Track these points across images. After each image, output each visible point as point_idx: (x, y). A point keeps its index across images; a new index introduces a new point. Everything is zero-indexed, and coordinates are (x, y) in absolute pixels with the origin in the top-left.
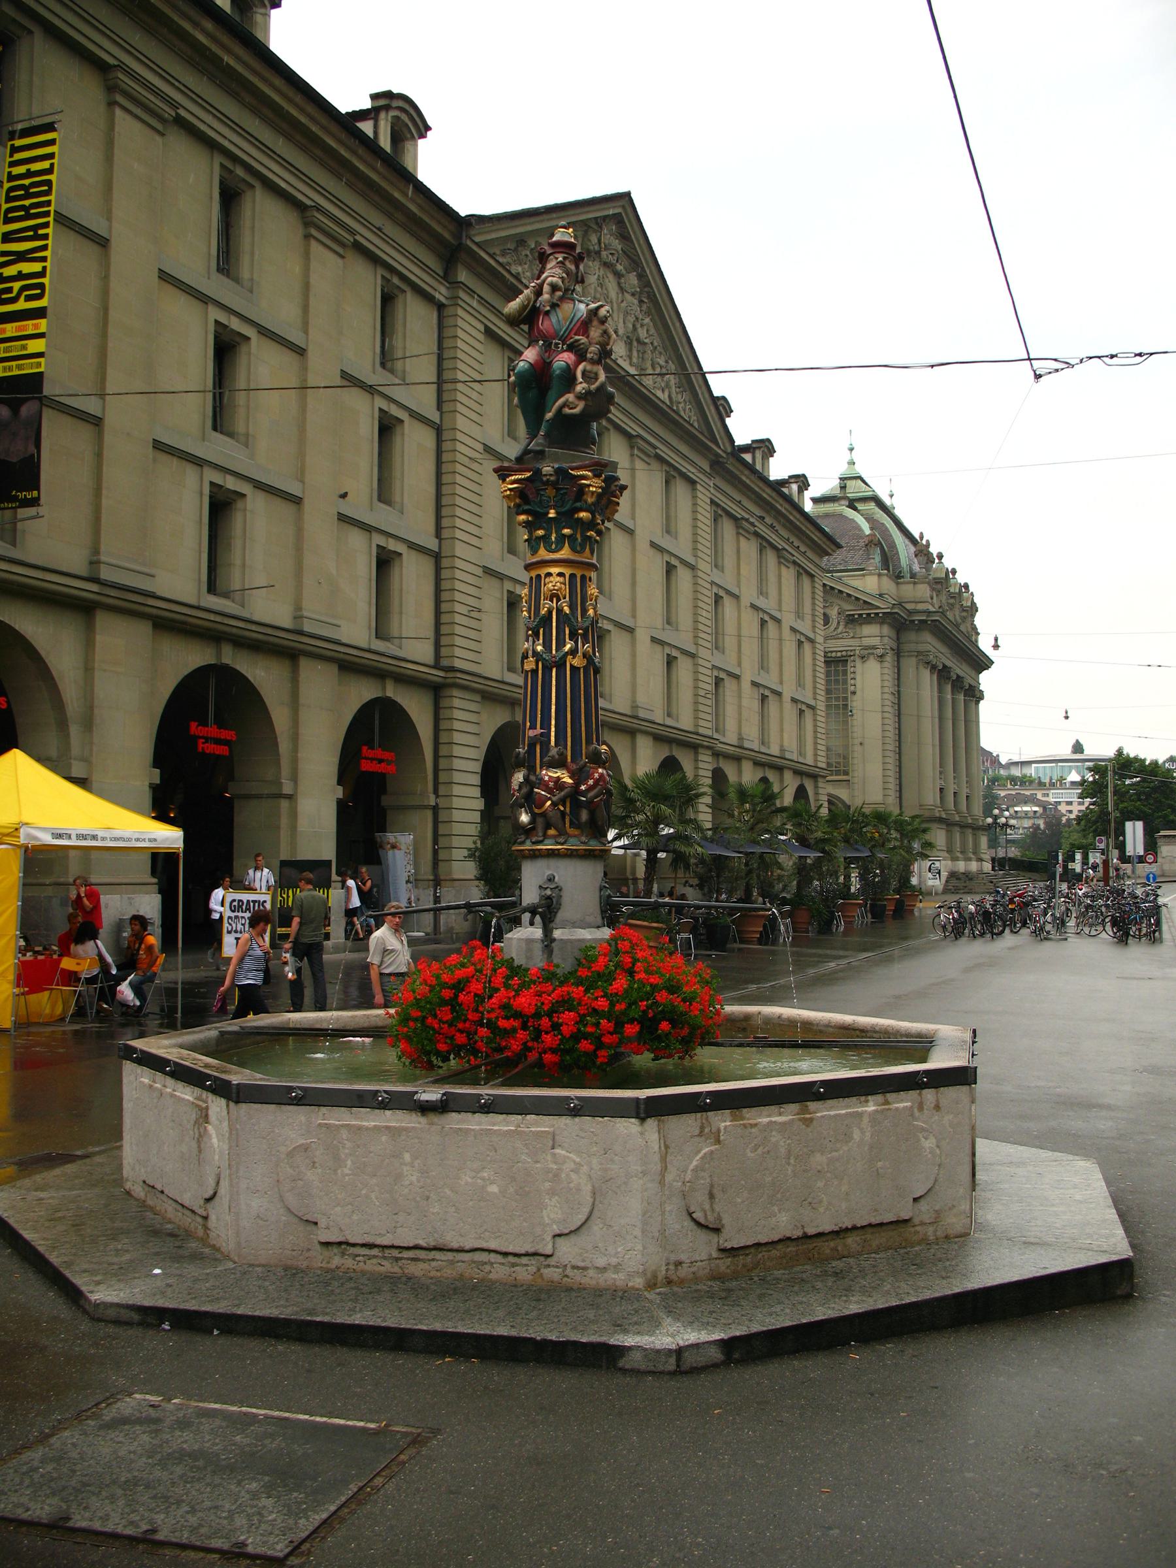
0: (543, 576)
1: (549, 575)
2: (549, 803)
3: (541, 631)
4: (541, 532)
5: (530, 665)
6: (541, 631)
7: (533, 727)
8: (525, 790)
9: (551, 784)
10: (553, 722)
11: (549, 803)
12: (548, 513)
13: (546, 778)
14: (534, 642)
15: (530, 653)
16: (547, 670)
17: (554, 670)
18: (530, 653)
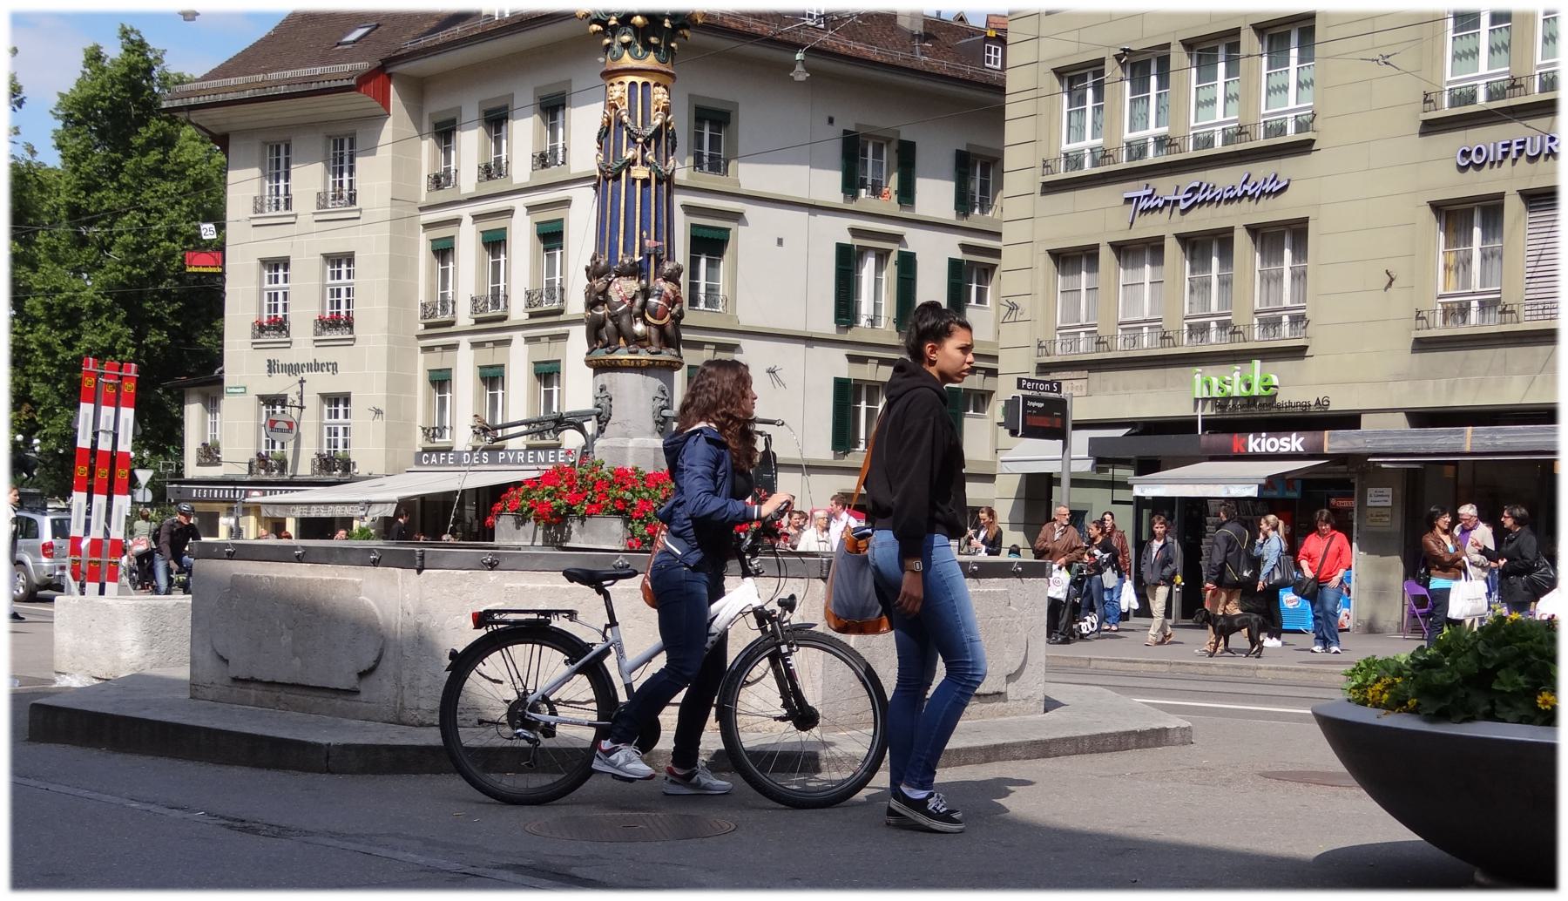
0: (652, 84)
1: (657, 85)
2: (668, 316)
3: (653, 143)
4: (653, 40)
5: (640, 172)
6: (653, 143)
7: (649, 237)
8: (638, 302)
9: (672, 297)
10: (665, 238)
11: (668, 316)
12: (664, 22)
13: (668, 291)
14: (644, 151)
15: (639, 161)
16: (659, 181)
17: (665, 185)
18: (639, 161)
